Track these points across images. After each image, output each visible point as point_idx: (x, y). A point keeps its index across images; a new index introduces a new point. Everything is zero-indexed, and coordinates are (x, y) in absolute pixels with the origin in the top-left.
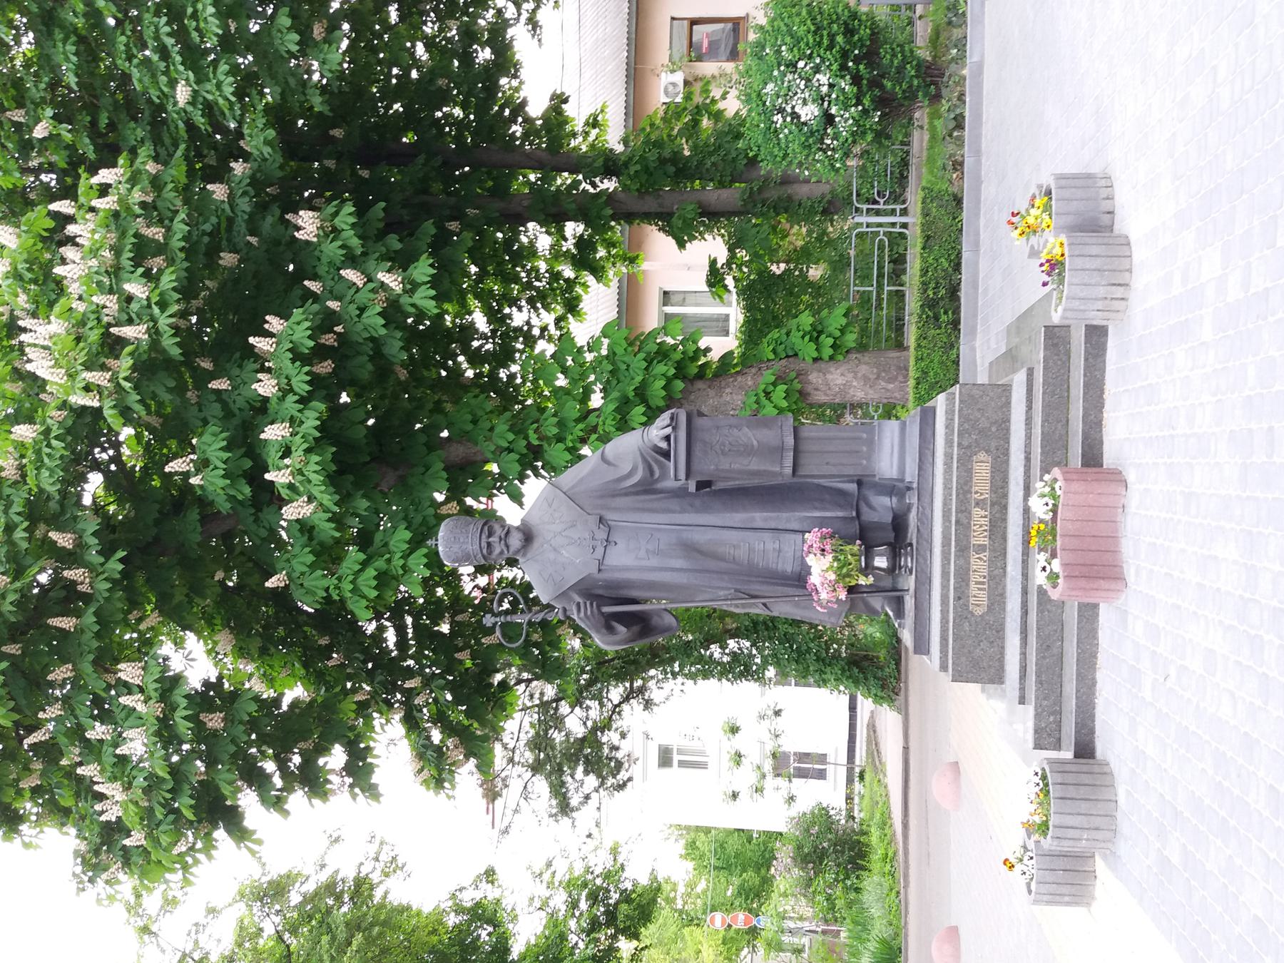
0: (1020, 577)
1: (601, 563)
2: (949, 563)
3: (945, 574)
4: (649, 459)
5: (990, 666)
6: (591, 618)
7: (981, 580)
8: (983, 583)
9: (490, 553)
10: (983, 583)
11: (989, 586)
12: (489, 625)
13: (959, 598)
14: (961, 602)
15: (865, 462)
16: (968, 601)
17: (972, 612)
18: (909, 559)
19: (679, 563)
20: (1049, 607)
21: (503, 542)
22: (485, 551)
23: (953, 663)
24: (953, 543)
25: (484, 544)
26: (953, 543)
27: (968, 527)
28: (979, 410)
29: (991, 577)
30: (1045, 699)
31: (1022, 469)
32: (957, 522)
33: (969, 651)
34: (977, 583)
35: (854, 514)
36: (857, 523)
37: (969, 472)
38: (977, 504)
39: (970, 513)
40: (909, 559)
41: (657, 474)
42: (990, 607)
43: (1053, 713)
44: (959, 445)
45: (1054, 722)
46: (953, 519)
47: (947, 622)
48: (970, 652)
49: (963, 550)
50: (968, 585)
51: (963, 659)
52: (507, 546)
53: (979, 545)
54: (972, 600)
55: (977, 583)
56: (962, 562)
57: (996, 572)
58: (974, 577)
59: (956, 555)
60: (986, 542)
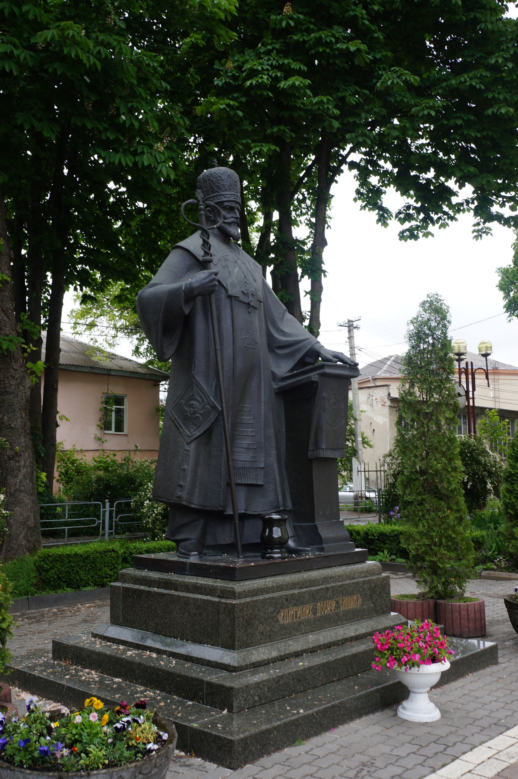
0: (311, 646)
1: (236, 298)
2: (301, 588)
3: (293, 586)
4: (296, 347)
5: (248, 635)
6: (211, 284)
7: (298, 616)
8: (296, 617)
9: (225, 208)
10: (296, 617)
11: (295, 623)
12: (197, 195)
13: (287, 600)
14: (285, 602)
15: (321, 513)
16: (285, 608)
17: (279, 612)
18: (279, 555)
19: (239, 364)
20: (322, 673)
21: (235, 220)
22: (226, 204)
23: (248, 603)
24: (316, 588)
25: (234, 205)
26: (316, 588)
27: (326, 599)
28: (380, 593)
29: (300, 624)
30: (268, 688)
31: (364, 631)
32: (327, 589)
33: (256, 616)
34: (296, 612)
35: (282, 508)
36: (272, 511)
37: (352, 594)
38: (337, 603)
39: (333, 598)
40: (279, 555)
41: (278, 351)
42: (283, 627)
43: (260, 698)
44: (364, 582)
45: (255, 701)
46: (329, 586)
47: (267, 593)
48: (256, 616)
49: (314, 597)
50: (295, 605)
51: (251, 611)
52: (229, 224)
53: (316, 609)
54: (286, 610)
55: (296, 612)
56: (307, 597)
57: (303, 626)
58: (299, 610)
59: (311, 591)
60: (319, 615)
